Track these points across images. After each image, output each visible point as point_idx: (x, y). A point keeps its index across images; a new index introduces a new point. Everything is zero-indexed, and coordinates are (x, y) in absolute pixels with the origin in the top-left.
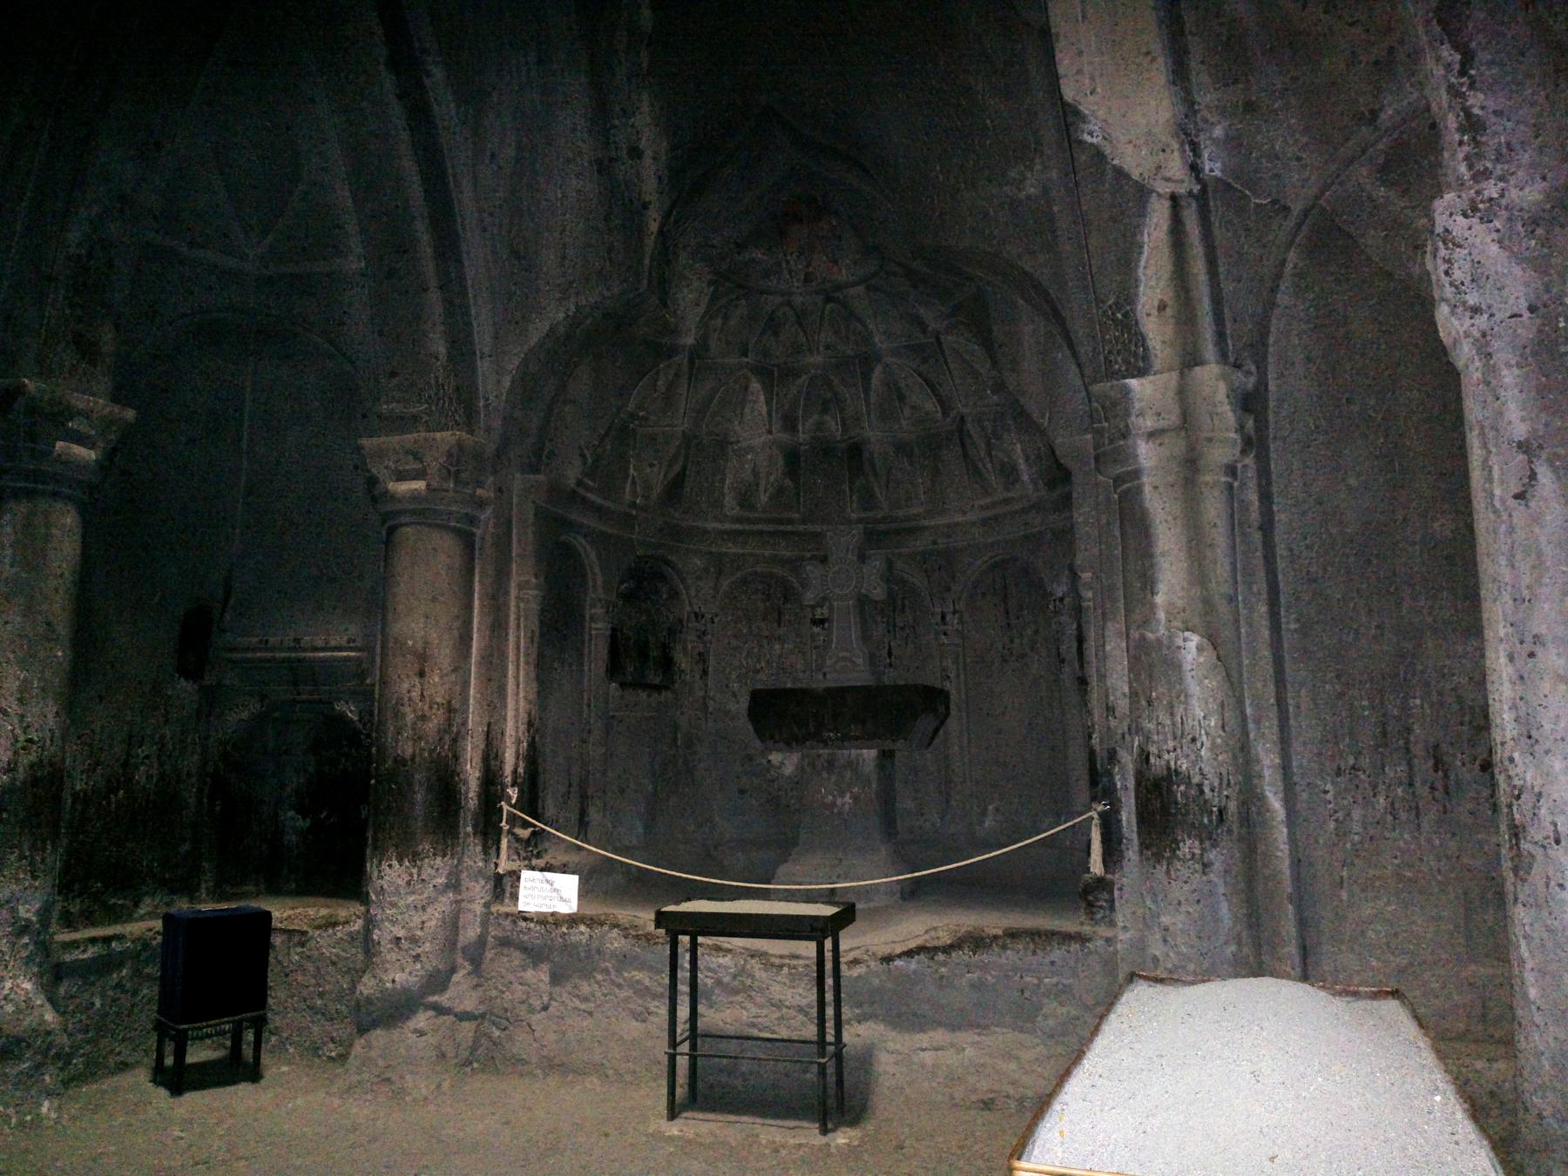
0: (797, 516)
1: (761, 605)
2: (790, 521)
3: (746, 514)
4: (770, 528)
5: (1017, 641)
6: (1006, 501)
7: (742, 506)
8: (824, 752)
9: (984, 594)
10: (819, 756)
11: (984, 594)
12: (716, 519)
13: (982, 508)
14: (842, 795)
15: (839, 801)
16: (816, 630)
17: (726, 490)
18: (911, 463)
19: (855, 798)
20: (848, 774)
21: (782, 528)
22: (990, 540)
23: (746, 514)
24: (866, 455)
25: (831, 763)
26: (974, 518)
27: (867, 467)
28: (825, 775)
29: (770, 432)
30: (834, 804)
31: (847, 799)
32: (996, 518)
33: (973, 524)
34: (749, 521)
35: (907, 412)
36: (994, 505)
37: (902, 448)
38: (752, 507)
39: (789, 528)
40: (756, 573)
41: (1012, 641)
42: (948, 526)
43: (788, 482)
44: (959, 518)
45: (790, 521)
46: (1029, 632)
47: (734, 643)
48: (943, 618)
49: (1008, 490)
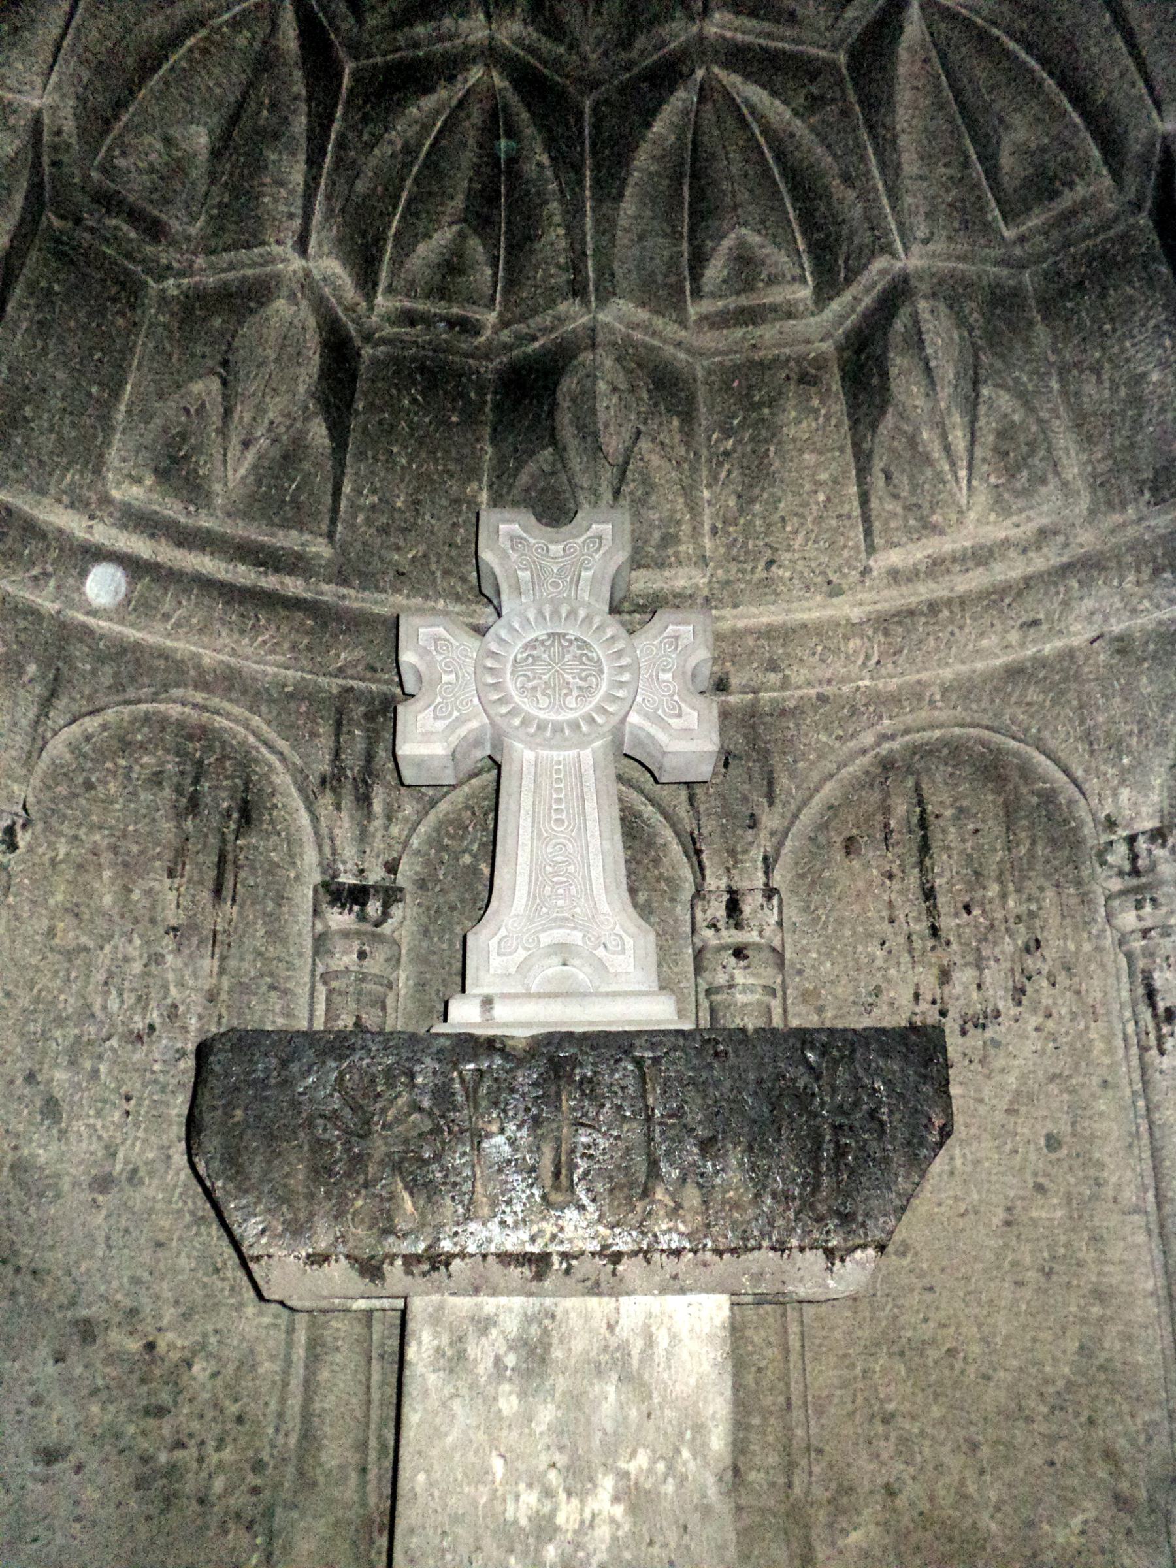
0: (320, 549)
1: (167, 826)
2: (296, 564)
3: (172, 509)
4: (244, 575)
5: (963, 977)
6: (981, 556)
7: (162, 474)
8: (510, 1309)
9: (850, 846)
10: (484, 1324)
11: (850, 846)
12: (77, 503)
13: (894, 575)
14: (579, 1479)
15: (567, 1514)
16: (339, 919)
17: (120, 416)
18: (688, 436)
19: (635, 1497)
20: (609, 1396)
21: (270, 582)
22: (893, 684)
23: (172, 509)
24: (568, 384)
25: (535, 1355)
26: (856, 614)
27: (565, 419)
28: (509, 1403)
29: (302, 245)
30: (545, 1528)
31: (603, 1500)
32: (933, 607)
33: (854, 629)
34: (186, 538)
35: (715, 271)
36: (936, 567)
37: (665, 387)
38: (194, 489)
39: (293, 586)
40: (163, 723)
41: (945, 976)
42: (769, 633)
43: (318, 432)
44: (813, 610)
45: (296, 564)
46: (1008, 946)
47: (69, 934)
48: (733, 907)
49: (1000, 506)
